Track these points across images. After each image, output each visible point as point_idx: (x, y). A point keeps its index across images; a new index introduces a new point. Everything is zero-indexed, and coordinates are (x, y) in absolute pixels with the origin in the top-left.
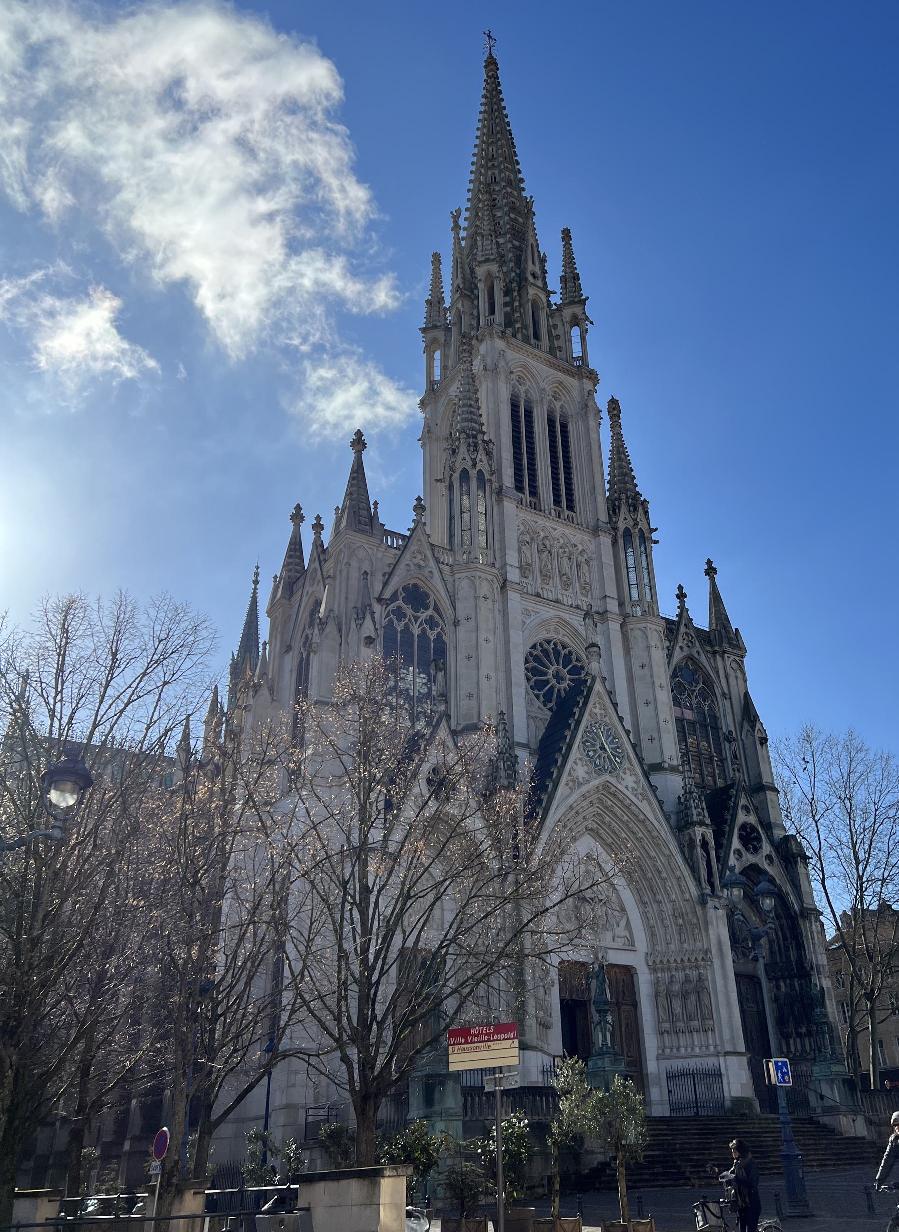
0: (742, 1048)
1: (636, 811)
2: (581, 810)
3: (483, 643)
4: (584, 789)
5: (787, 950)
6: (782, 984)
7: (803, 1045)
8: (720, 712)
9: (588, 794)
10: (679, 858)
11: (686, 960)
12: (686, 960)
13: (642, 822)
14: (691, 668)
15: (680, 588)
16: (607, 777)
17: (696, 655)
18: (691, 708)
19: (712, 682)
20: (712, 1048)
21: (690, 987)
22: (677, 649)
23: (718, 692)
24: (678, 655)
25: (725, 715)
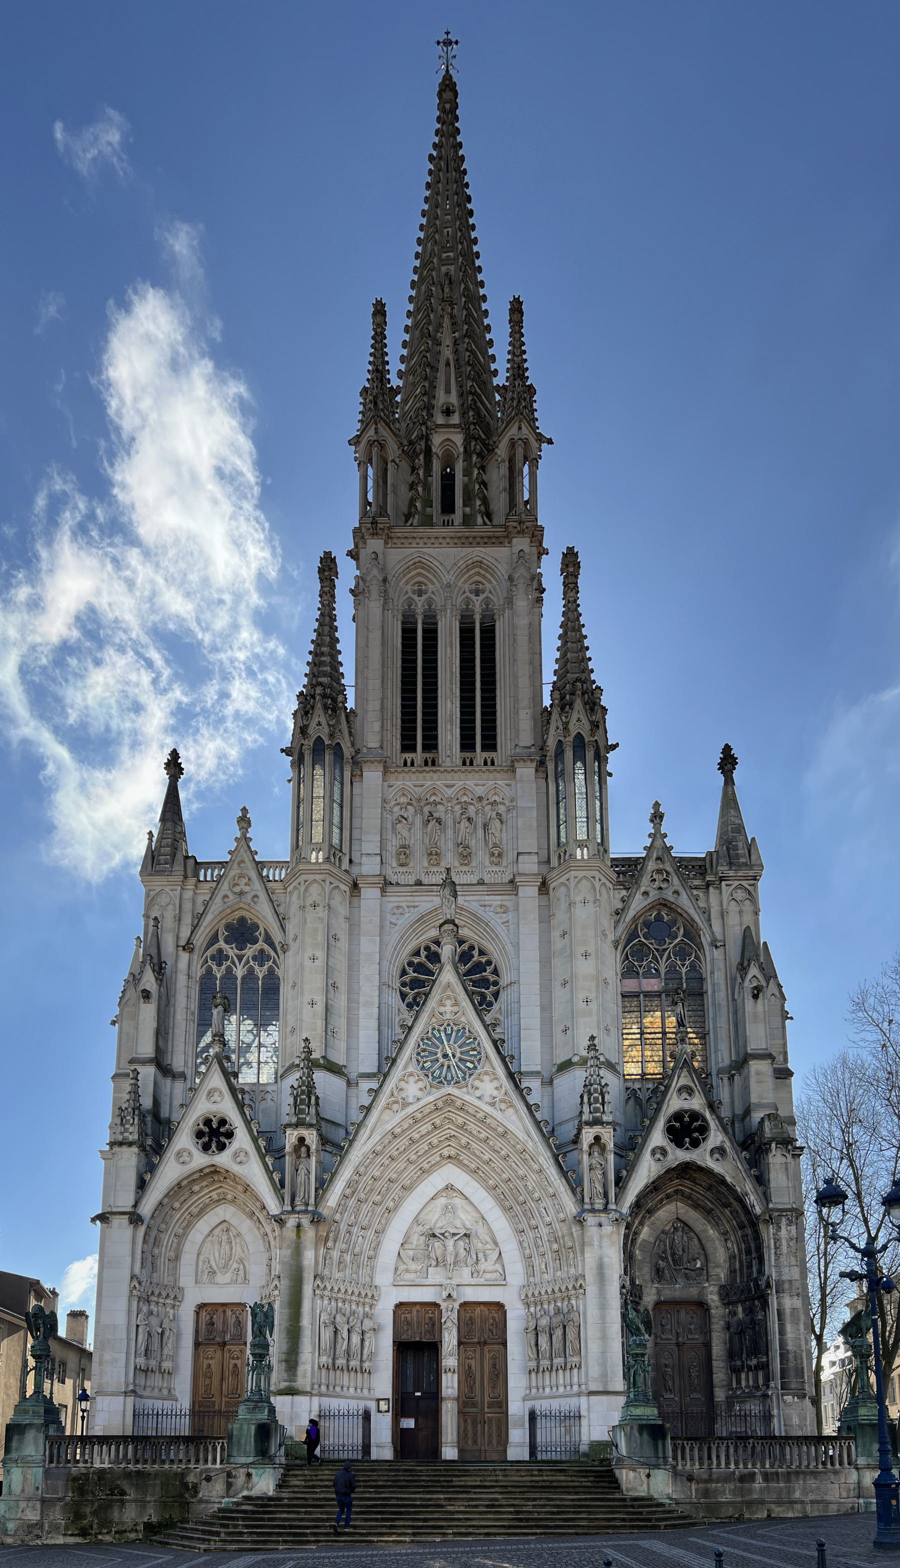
0: (619, 1384)
1: (494, 1124)
3: (308, 963)
4: (410, 1110)
5: (750, 1266)
6: (740, 1309)
7: (756, 1380)
8: (706, 969)
9: (419, 1116)
10: (552, 1172)
11: (556, 1290)
12: (556, 1290)
14: (666, 918)
17: (671, 898)
19: (698, 930)
20: (575, 1388)
21: (556, 1320)
22: (639, 896)
23: (706, 940)
24: (638, 903)
25: (712, 973)
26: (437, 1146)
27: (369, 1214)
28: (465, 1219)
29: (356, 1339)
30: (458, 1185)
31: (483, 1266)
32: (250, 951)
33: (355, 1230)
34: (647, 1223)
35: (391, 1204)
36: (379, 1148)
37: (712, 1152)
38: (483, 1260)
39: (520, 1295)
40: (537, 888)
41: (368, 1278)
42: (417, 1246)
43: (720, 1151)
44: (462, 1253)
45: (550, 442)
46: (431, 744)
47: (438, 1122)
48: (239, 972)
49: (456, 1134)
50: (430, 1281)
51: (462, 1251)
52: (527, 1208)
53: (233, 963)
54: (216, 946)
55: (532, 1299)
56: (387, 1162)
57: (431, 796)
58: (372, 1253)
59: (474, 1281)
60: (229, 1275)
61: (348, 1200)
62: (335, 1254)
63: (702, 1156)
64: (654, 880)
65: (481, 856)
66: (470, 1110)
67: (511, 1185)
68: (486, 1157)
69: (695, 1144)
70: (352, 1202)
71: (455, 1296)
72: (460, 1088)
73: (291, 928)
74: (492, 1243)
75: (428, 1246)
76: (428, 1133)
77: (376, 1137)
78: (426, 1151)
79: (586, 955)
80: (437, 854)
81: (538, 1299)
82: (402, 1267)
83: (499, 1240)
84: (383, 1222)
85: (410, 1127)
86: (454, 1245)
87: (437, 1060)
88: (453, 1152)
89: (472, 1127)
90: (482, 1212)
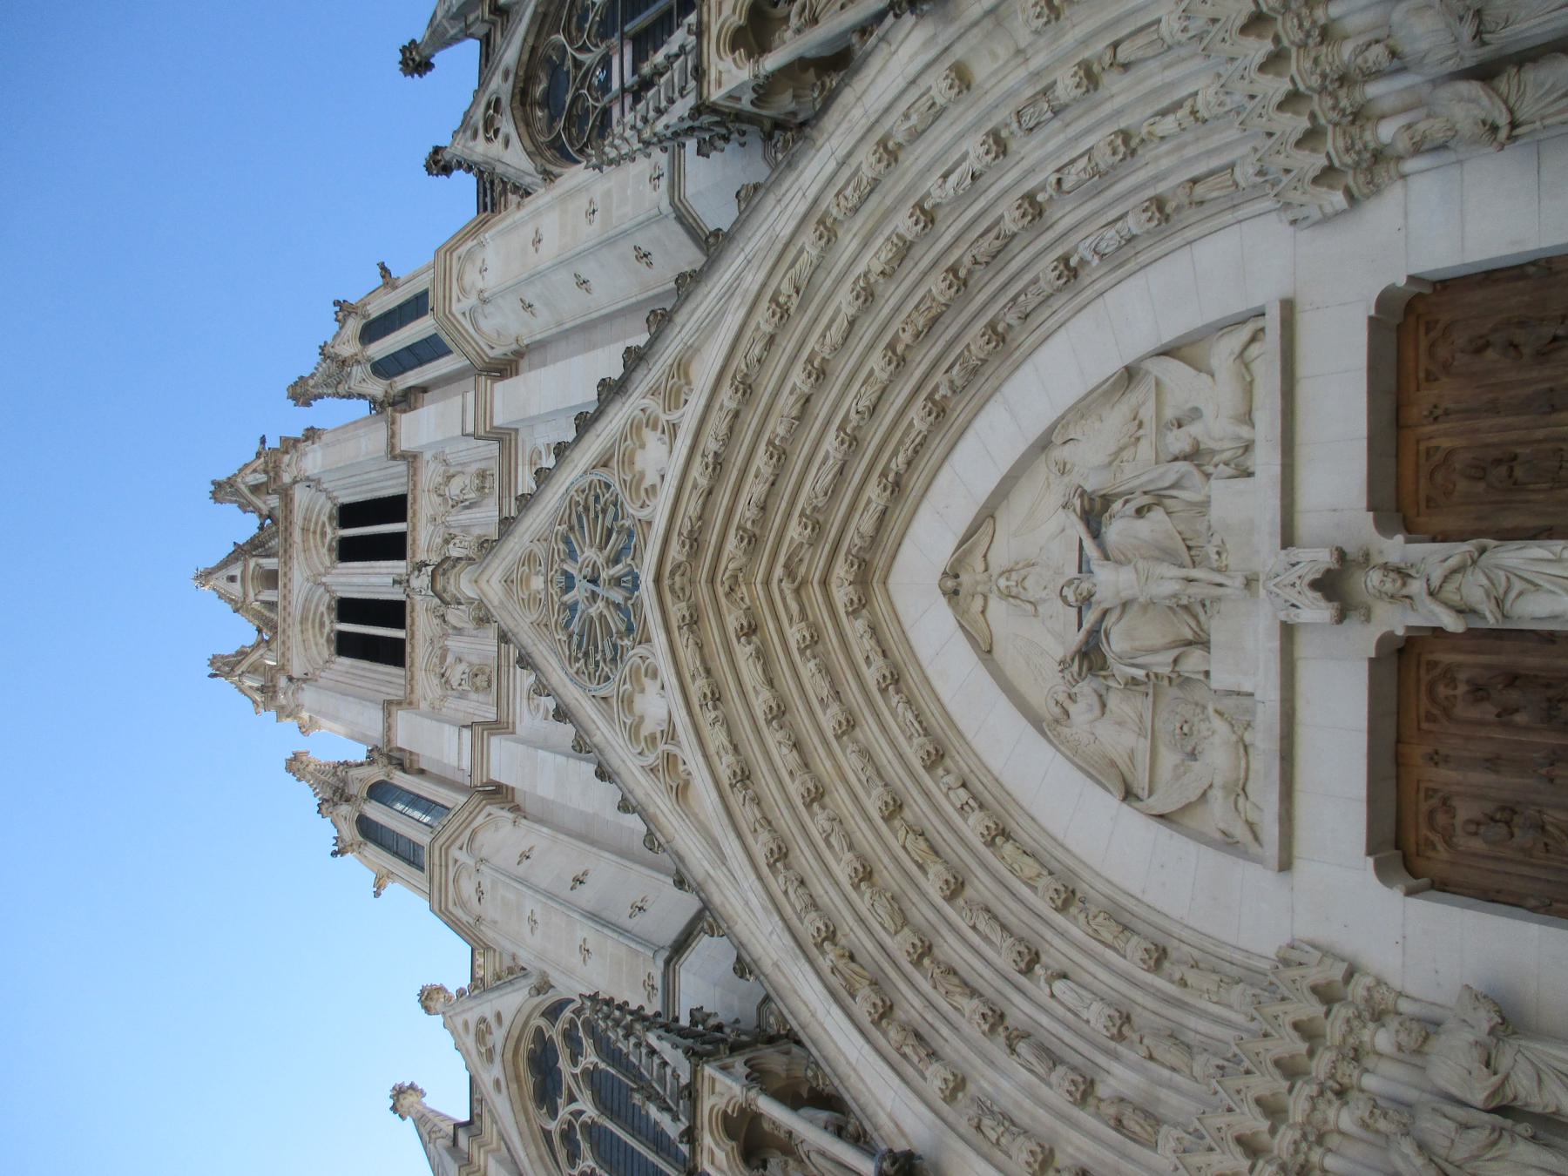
1: (718, 424)
13: (747, 389)
18: (606, 62)
27: (981, 926)
31: (1216, 429)
35: (973, 826)
38: (1195, 429)
39: (1326, 219)
41: (1236, 993)
42: (1141, 733)
44: (1156, 525)
45: (263, 441)
47: (733, 620)
49: (782, 559)
51: (1143, 528)
52: (967, 261)
55: (1333, 142)
56: (821, 817)
58: (1135, 946)
59: (1267, 461)
61: (899, 1014)
67: (906, 337)
71: (1324, 559)
74: (1133, 398)
75: (1134, 681)
76: (762, 656)
77: (731, 846)
78: (826, 670)
79: (537, 241)
81: (1321, 106)
83: (1115, 365)
84: (1030, 867)
88: (841, 570)
90: (1022, 447)
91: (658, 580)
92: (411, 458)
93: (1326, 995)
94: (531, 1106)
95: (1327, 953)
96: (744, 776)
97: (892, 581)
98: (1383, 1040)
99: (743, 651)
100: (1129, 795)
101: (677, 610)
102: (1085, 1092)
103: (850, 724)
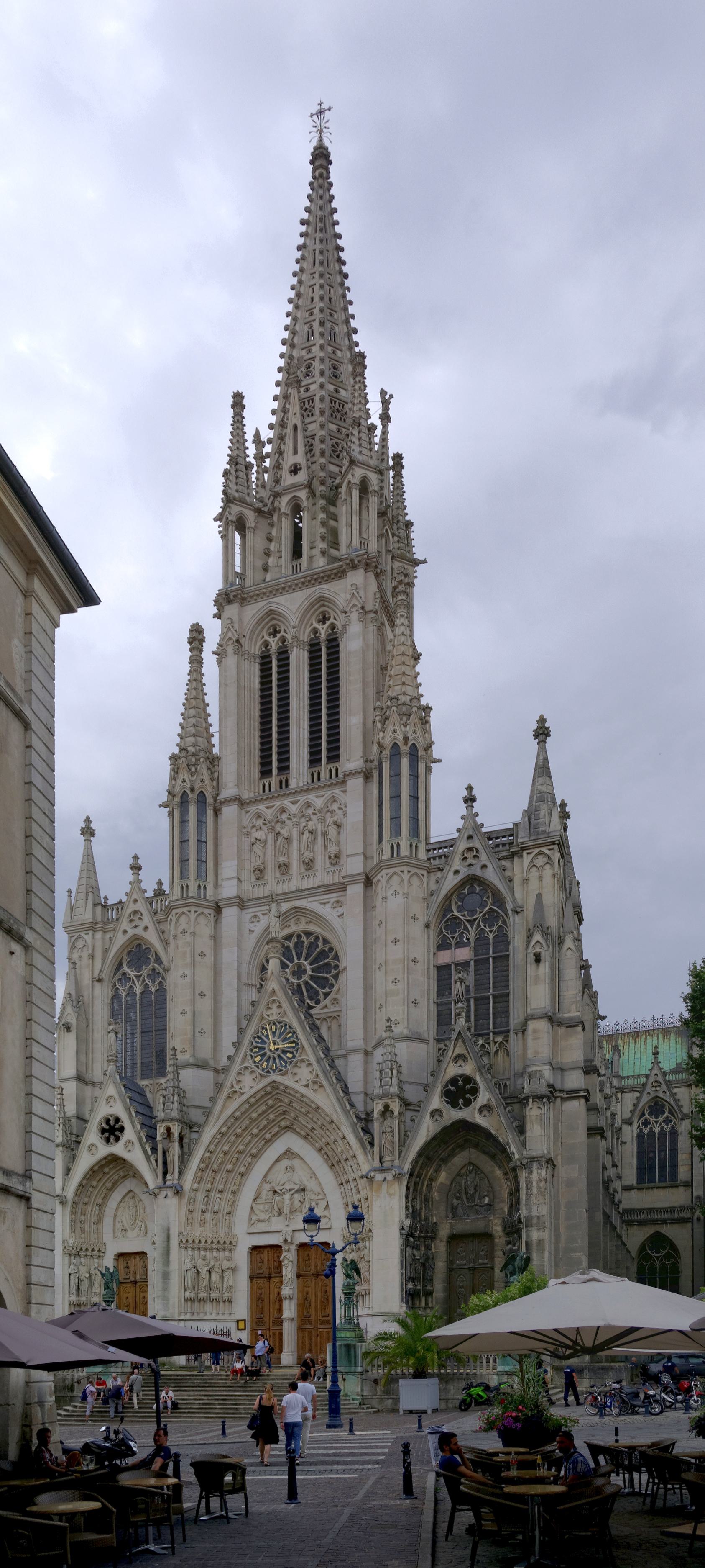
2: (254, 1115)
9: (253, 1100)
15: (470, 788)
16: (274, 1077)
26: (274, 1120)
28: (301, 1176)
29: (215, 1277)
30: (295, 1149)
32: (145, 972)
33: (212, 1194)
34: (443, 1167)
35: (242, 1169)
36: (224, 1129)
37: (481, 1110)
40: (361, 885)
43: (486, 1108)
46: (284, 768)
48: (138, 990)
50: (273, 1228)
53: (134, 982)
54: (121, 971)
57: (281, 813)
58: (228, 1209)
60: (136, 1230)
62: (197, 1215)
63: (472, 1114)
64: (466, 858)
65: (321, 861)
66: (291, 1092)
68: (310, 1127)
69: (468, 1103)
70: (208, 1174)
72: (283, 1075)
73: (171, 948)
76: (264, 1112)
77: (221, 1121)
78: (265, 1127)
79: (395, 941)
80: (285, 865)
82: (254, 1218)
84: (238, 1183)
85: (247, 1110)
86: (291, 1199)
87: (265, 1054)
88: (288, 1123)
89: (295, 1105)
91: (274, 1082)
92: (344, 782)
93: (231, 1243)
94: (126, 951)
95: (237, 1242)
96: (236, 1119)
97: (289, 1133)
98: (227, 1253)
99: (264, 1108)
100: (255, 1200)
101: (269, 1089)
102: (203, 1212)
103: (256, 1136)
